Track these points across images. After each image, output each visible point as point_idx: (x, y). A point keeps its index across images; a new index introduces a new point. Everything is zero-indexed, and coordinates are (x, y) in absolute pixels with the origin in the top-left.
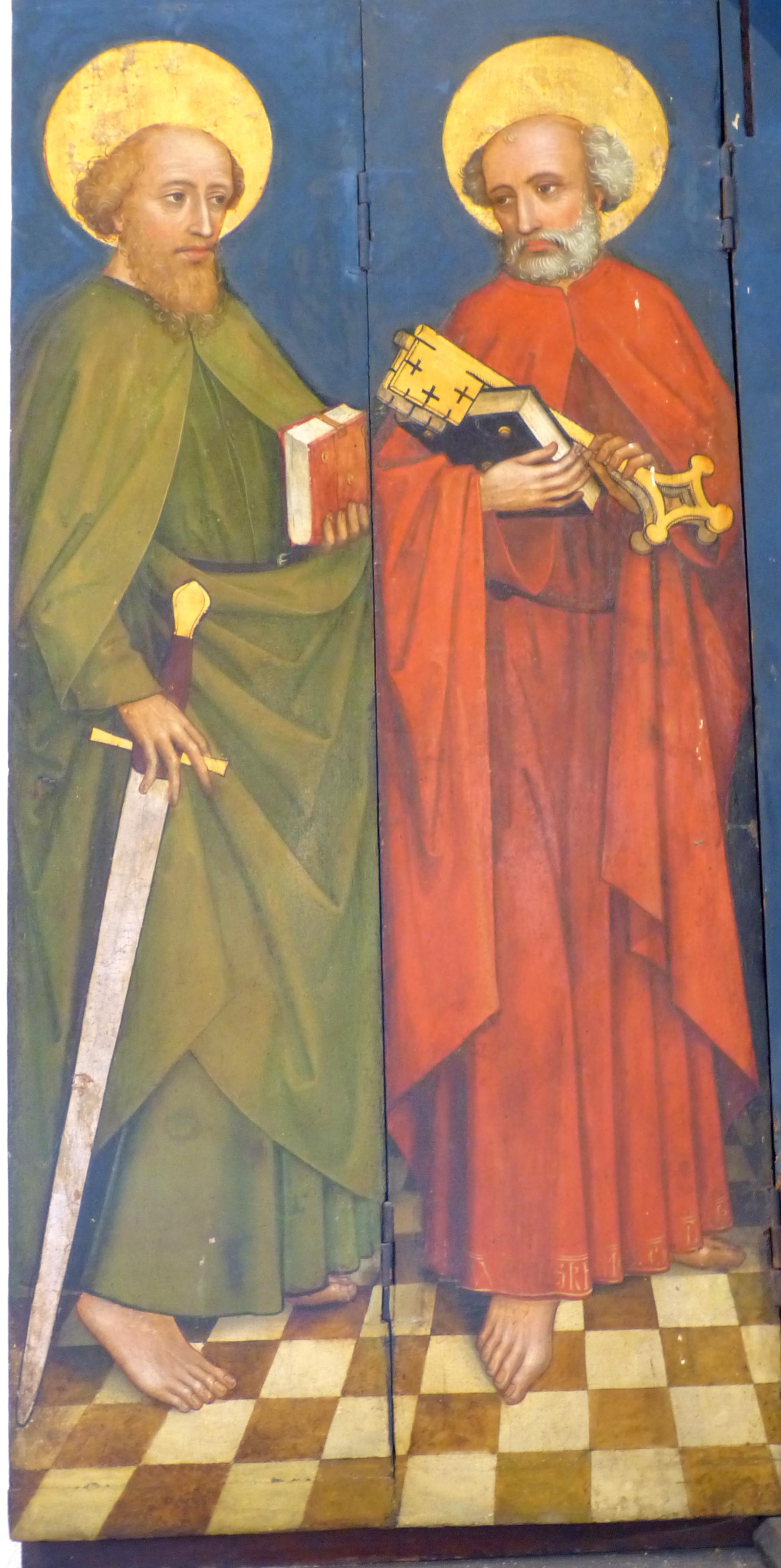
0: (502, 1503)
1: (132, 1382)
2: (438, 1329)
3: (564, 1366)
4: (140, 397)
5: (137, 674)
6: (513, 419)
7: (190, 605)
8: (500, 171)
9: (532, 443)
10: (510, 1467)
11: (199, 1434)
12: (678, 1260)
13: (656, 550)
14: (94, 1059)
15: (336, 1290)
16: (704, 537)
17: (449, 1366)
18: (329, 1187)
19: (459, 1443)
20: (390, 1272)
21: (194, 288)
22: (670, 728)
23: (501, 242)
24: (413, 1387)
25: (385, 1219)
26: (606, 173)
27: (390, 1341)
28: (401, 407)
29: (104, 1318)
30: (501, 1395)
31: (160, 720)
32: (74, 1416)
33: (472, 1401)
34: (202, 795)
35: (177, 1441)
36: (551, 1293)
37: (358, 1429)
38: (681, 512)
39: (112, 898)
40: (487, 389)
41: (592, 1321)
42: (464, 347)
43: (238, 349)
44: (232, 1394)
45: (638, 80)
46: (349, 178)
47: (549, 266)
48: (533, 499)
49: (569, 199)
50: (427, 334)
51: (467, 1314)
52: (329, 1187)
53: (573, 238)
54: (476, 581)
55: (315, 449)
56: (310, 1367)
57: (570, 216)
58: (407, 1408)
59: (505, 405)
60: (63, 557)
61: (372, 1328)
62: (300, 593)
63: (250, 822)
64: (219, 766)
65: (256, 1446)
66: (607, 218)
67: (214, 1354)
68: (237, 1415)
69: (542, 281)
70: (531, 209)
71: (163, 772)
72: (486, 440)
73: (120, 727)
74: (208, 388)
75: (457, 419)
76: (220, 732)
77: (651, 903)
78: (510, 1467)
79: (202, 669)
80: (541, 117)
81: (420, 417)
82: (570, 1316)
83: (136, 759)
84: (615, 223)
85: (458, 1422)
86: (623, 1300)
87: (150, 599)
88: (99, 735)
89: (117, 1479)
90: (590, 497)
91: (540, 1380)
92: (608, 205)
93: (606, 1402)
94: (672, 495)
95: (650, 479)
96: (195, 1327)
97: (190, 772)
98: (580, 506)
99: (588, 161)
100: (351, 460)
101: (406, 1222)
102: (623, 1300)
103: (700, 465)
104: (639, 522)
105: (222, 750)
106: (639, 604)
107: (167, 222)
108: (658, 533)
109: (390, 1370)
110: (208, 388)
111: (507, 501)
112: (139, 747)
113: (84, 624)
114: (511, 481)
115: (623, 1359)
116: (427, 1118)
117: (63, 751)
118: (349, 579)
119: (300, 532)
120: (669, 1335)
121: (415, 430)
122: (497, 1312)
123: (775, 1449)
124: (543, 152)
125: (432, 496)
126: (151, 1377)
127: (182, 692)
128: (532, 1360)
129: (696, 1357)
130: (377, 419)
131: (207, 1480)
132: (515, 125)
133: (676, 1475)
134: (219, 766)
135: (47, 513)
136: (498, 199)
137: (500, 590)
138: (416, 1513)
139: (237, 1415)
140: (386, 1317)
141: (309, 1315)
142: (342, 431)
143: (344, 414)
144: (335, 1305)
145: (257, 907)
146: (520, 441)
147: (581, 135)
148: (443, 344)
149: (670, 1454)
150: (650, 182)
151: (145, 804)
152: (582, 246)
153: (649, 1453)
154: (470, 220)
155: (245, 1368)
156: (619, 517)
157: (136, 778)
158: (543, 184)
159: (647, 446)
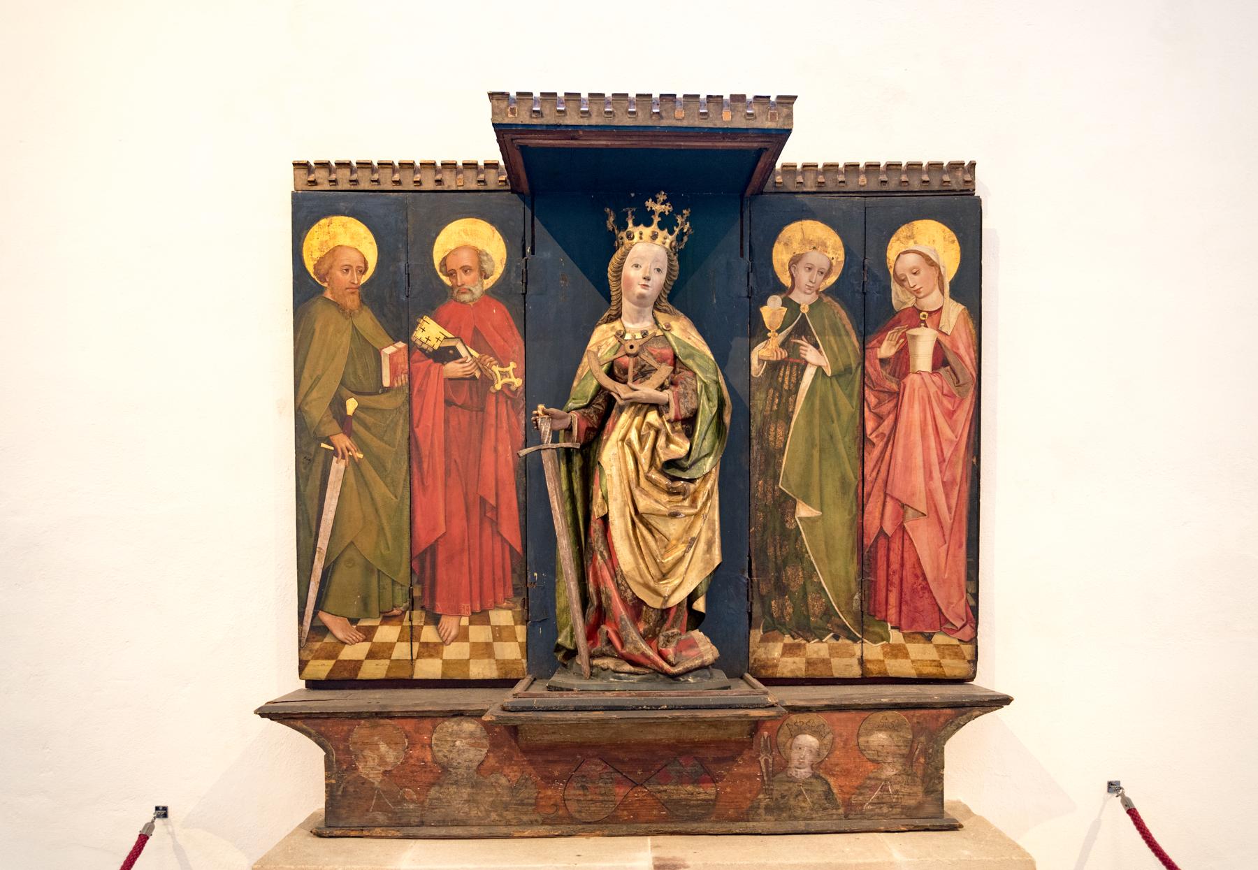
0: (443, 673)
1: (335, 636)
2: (426, 624)
3: (463, 635)
4: (335, 337)
5: (335, 426)
6: (454, 348)
7: (351, 405)
8: (451, 265)
9: (460, 357)
10: (446, 663)
11: (355, 651)
12: (497, 606)
13: (498, 392)
14: (323, 543)
15: (395, 612)
16: (513, 388)
17: (429, 634)
18: (394, 582)
19: (431, 656)
20: (412, 607)
21: (352, 301)
22: (500, 448)
23: (452, 288)
24: (418, 640)
25: (411, 592)
26: (485, 266)
27: (412, 627)
28: (419, 343)
29: (326, 618)
30: (444, 643)
31: (342, 441)
32: (317, 645)
33: (436, 644)
34: (355, 465)
35: (348, 653)
36: (459, 614)
37: (402, 651)
38: (506, 380)
39: (327, 495)
40: (446, 338)
41: (471, 623)
42: (439, 323)
43: (367, 322)
44: (364, 640)
45: (497, 235)
46: (402, 265)
47: (467, 297)
48: (460, 374)
49: (475, 274)
50: (427, 318)
51: (434, 620)
52: (394, 582)
53: (474, 287)
54: (441, 399)
55: (391, 356)
56: (386, 633)
57: (474, 281)
58: (416, 646)
59: (451, 343)
60: (311, 388)
61: (406, 623)
62: (383, 401)
63: (370, 473)
64: (361, 456)
65: (371, 655)
66: (485, 281)
67: (359, 629)
68: (366, 646)
69: (464, 302)
70: (462, 278)
71: (343, 457)
72: (444, 355)
73: (330, 443)
74: (356, 333)
75: (436, 347)
76: (362, 445)
77: (492, 501)
78: (446, 663)
79: (356, 426)
80: (465, 247)
81: (425, 346)
82: (465, 621)
83: (335, 453)
84: (488, 283)
85: (431, 650)
86: (480, 617)
87: (338, 404)
88: (323, 445)
89: (331, 663)
90: (478, 374)
91: (455, 639)
92: (486, 277)
93: (475, 646)
94: (504, 374)
95: (496, 369)
96: (353, 621)
97: (352, 457)
98: (474, 377)
99: (480, 262)
100: (402, 359)
101: (417, 593)
102: (480, 617)
103: (513, 365)
104: (492, 382)
105: (362, 451)
106: (491, 409)
107: (344, 279)
108: (498, 387)
109: (411, 635)
110: (356, 333)
111: (451, 375)
112: (336, 449)
113: (318, 411)
114: (453, 369)
115: (480, 634)
116: (424, 564)
117: (313, 449)
118: (401, 398)
119: (386, 383)
120: (493, 627)
121: (423, 350)
122: (443, 619)
123: (524, 661)
124: (466, 259)
125: (428, 372)
126: (340, 635)
127: (348, 432)
128: (453, 633)
129: (500, 634)
130: (412, 347)
131: (357, 664)
132: (457, 249)
133: (494, 667)
134: (361, 456)
135: (306, 374)
136: (451, 274)
137: (448, 403)
138: (418, 675)
139: (366, 646)
140: (410, 620)
141: (387, 619)
142: (400, 350)
143: (401, 345)
144: (395, 616)
145: (372, 499)
146: (457, 356)
147: (479, 254)
148: (432, 322)
149: (493, 661)
150: (498, 271)
151: (338, 467)
152: (477, 291)
153: (486, 661)
154: (441, 281)
155: (369, 633)
156: (488, 381)
157: (335, 459)
158: (466, 270)
159: (496, 358)
